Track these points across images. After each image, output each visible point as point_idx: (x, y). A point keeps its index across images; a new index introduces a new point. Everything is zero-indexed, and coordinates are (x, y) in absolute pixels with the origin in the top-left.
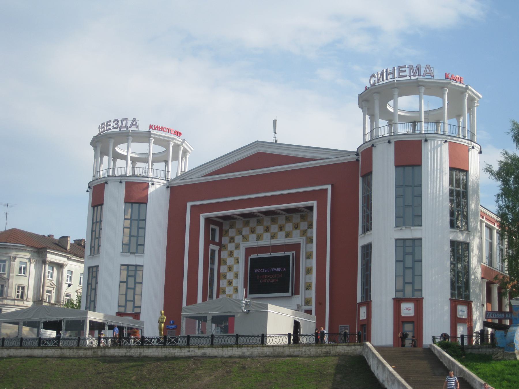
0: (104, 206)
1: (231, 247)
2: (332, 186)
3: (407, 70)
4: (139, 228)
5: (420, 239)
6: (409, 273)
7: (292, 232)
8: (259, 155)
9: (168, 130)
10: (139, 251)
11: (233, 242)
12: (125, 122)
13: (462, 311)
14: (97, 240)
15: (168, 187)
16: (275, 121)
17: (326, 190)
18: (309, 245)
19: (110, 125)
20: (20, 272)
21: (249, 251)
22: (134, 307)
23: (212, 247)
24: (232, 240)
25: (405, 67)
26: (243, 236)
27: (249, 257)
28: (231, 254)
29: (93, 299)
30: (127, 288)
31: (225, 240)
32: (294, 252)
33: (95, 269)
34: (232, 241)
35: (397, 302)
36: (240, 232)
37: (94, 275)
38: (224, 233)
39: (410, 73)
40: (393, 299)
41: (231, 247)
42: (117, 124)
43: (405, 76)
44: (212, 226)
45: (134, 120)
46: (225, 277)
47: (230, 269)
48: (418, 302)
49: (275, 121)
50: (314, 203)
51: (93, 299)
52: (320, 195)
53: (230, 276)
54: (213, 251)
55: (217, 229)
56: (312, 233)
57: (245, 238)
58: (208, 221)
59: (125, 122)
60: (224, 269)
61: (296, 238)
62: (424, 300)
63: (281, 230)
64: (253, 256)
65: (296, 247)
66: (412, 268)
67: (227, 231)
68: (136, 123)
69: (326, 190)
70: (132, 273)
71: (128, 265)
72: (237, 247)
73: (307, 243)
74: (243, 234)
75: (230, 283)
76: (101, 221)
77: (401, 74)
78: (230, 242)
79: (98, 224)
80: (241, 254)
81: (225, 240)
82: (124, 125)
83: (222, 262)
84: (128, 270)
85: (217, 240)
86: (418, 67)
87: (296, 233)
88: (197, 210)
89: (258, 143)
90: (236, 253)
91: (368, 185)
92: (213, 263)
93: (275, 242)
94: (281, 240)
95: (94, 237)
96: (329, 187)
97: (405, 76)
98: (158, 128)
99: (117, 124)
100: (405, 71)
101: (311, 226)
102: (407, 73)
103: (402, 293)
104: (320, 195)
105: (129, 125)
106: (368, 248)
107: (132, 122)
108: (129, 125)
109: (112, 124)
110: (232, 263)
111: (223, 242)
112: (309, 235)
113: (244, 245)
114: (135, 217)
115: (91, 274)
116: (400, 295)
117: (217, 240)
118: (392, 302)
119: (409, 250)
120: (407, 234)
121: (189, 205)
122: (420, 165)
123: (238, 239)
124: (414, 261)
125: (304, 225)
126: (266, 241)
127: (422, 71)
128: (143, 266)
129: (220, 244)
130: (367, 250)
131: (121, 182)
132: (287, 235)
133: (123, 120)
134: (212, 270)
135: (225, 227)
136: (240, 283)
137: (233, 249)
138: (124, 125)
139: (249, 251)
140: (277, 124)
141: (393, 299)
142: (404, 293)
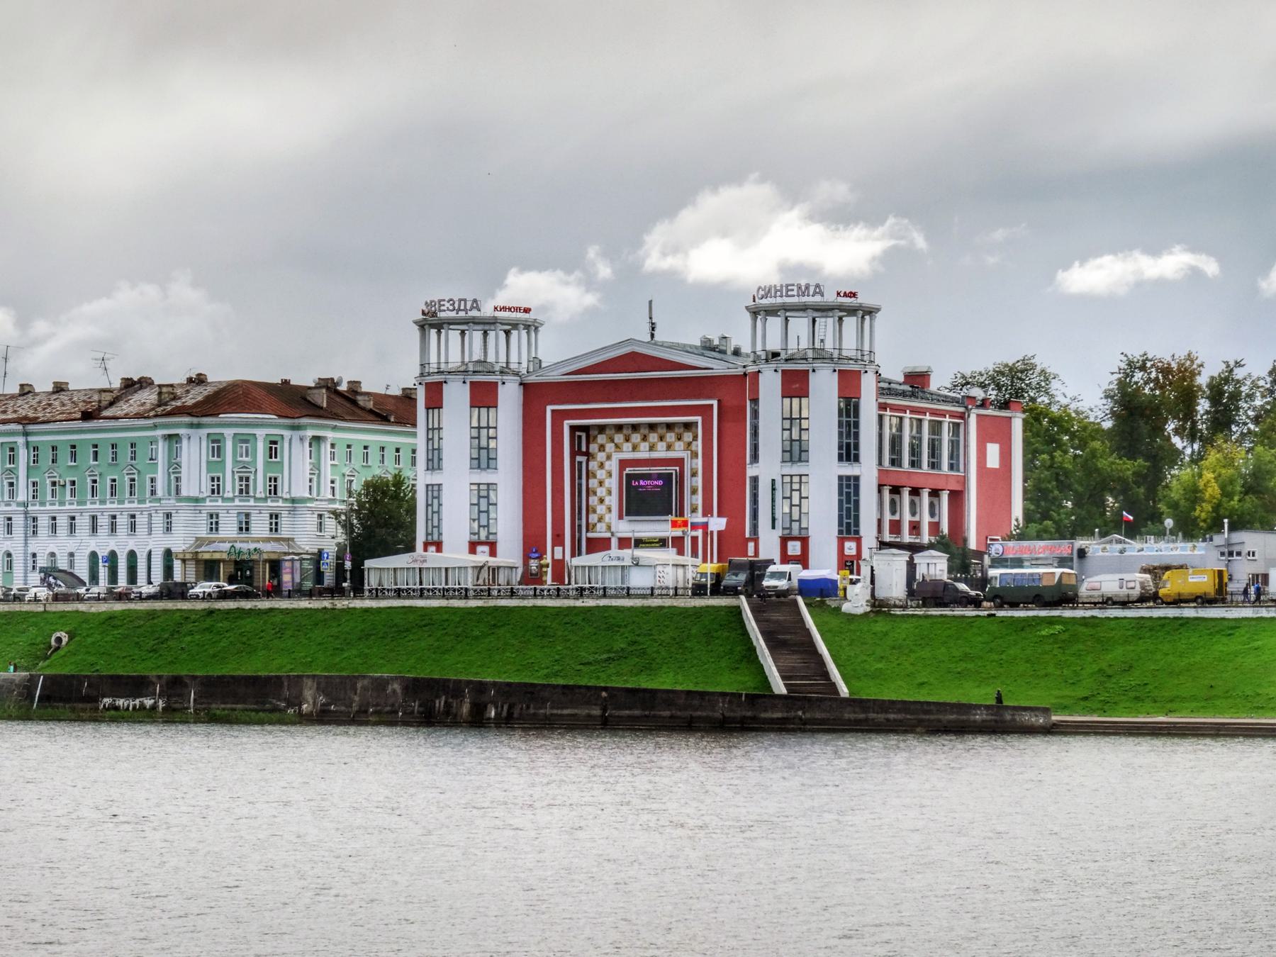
0: (444, 411)
1: (601, 456)
2: (719, 401)
3: (795, 288)
7: (674, 443)
8: (633, 355)
9: (517, 309)
11: (604, 451)
12: (463, 302)
13: (850, 548)
14: (436, 452)
15: (521, 384)
16: (650, 302)
17: (712, 405)
18: (694, 461)
19: (444, 305)
20: (271, 457)
21: (623, 464)
22: (489, 533)
23: (579, 458)
24: (602, 448)
25: (793, 285)
26: (616, 444)
27: (625, 473)
28: (602, 466)
29: (436, 524)
30: (480, 512)
31: (594, 448)
32: (677, 468)
33: (436, 488)
34: (602, 449)
35: (784, 541)
36: (612, 440)
37: (436, 494)
38: (591, 439)
39: (798, 292)
43: (794, 296)
44: (578, 433)
45: (475, 301)
46: (595, 493)
48: (804, 541)
49: (650, 302)
50: (699, 419)
51: (436, 524)
53: (601, 492)
54: (580, 463)
55: (584, 435)
56: (697, 446)
58: (573, 429)
59: (463, 302)
60: (593, 483)
61: (679, 452)
63: (661, 440)
64: (628, 470)
65: (679, 462)
67: (595, 437)
68: (477, 304)
69: (712, 405)
70: (484, 493)
71: (479, 484)
72: (609, 458)
73: (692, 458)
74: (616, 441)
75: (602, 501)
76: (439, 429)
77: (790, 293)
78: (600, 451)
79: (436, 431)
80: (613, 465)
81: (594, 448)
82: (462, 307)
83: (590, 475)
84: (479, 490)
85: (584, 449)
86: (807, 287)
87: (679, 445)
88: (559, 416)
90: (607, 464)
91: (755, 414)
92: (580, 478)
93: (655, 455)
94: (661, 453)
95: (430, 448)
96: (715, 403)
97: (794, 296)
98: (504, 309)
100: (793, 290)
101: (695, 438)
102: (795, 293)
105: (468, 308)
106: (755, 480)
107: (472, 305)
108: (468, 308)
109: (447, 305)
110: (604, 477)
111: (591, 450)
112: (694, 448)
113: (616, 457)
114: (484, 424)
115: (430, 493)
117: (584, 449)
119: (796, 486)
121: (549, 408)
123: (610, 447)
126: (643, 454)
128: (496, 484)
129: (588, 454)
130: (755, 482)
131: (464, 382)
132: (669, 447)
133: (460, 300)
134: (580, 485)
135: (593, 433)
136: (613, 501)
137: (604, 459)
138: (462, 307)
139: (623, 464)
140: (653, 303)
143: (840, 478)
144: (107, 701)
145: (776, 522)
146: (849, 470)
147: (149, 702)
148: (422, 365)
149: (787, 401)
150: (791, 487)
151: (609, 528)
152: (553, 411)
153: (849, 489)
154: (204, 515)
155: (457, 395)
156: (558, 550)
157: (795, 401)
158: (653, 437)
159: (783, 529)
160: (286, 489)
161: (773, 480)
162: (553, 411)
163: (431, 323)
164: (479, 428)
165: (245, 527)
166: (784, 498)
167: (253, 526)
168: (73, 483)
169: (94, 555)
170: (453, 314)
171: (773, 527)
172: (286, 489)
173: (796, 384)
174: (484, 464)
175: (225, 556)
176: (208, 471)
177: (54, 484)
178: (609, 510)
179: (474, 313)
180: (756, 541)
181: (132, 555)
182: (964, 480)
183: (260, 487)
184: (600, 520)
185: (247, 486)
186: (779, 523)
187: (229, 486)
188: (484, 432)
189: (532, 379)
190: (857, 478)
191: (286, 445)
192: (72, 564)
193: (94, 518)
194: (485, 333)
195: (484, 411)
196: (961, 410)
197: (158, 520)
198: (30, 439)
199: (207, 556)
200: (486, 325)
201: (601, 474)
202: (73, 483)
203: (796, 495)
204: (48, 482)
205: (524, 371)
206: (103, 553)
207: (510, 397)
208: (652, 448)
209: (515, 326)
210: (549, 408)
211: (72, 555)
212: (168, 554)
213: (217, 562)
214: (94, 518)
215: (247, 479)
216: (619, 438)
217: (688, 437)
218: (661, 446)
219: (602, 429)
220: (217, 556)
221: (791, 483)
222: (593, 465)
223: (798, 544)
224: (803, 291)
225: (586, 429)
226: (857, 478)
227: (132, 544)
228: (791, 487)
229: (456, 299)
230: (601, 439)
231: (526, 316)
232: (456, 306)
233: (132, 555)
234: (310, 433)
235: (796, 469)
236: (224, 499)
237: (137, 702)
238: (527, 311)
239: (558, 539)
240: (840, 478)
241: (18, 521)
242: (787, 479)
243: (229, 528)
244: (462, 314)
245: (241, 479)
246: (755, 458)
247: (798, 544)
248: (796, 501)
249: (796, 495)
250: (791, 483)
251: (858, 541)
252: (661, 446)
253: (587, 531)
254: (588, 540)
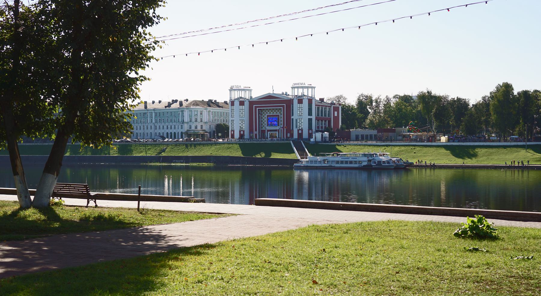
1: (264, 114)
16: (273, 86)
21: (268, 116)
23: (260, 115)
24: (264, 113)
28: (264, 116)
31: (262, 113)
35: (298, 130)
41: (264, 114)
45: (240, 86)
47: (264, 120)
48: (302, 130)
49: (273, 86)
50: (282, 108)
52: (283, 106)
54: (260, 116)
57: (267, 113)
65: (278, 116)
67: (262, 111)
70: (242, 122)
72: (265, 115)
80: (266, 116)
81: (262, 113)
87: (278, 112)
89: (269, 93)
90: (265, 116)
91: (293, 107)
93: (274, 114)
96: (285, 105)
98: (245, 87)
101: (281, 111)
104: (283, 106)
106: (293, 119)
113: (267, 115)
114: (242, 109)
119: (300, 120)
121: (254, 106)
123: (265, 113)
125: (280, 111)
127: (303, 84)
132: (276, 113)
139: (268, 116)
143: (309, 119)
144: (174, 161)
146: (310, 117)
147: (182, 161)
148: (230, 98)
149: (299, 104)
151: (265, 128)
152: (255, 106)
153: (310, 120)
154: (189, 126)
155: (237, 103)
156: (256, 132)
157: (300, 104)
158: (273, 111)
160: (204, 120)
161: (296, 119)
162: (255, 106)
163: (231, 90)
165: (196, 127)
167: (198, 128)
168: (163, 119)
169: (167, 133)
170: (236, 88)
172: (204, 120)
173: (300, 101)
175: (193, 133)
176: (189, 117)
177: (160, 120)
178: (265, 124)
179: (240, 88)
180: (293, 130)
181: (175, 133)
182: (331, 119)
183: (199, 120)
184: (264, 126)
185: (196, 120)
187: (193, 120)
189: (251, 100)
190: (312, 119)
191: (204, 112)
192: (163, 134)
193: (167, 126)
194: (242, 92)
196: (330, 105)
197: (180, 127)
198: (155, 111)
199: (189, 133)
200: (242, 90)
201: (264, 118)
202: (163, 119)
203: (300, 122)
204: (159, 119)
205: (249, 99)
206: (169, 133)
207: (247, 104)
208: (273, 113)
209: (248, 90)
210: (254, 106)
211: (163, 133)
212: (182, 133)
213: (191, 134)
214: (167, 126)
215: (197, 119)
216: (267, 111)
217: (280, 111)
218: (275, 113)
219: (264, 109)
220: (191, 133)
222: (262, 116)
223: (301, 131)
224: (302, 84)
225: (261, 109)
226: (312, 119)
227: (175, 131)
230: (264, 111)
231: (249, 88)
233: (175, 133)
234: (208, 110)
236: (192, 123)
237: (180, 161)
238: (249, 87)
239: (256, 130)
240: (309, 119)
241: (153, 127)
242: (299, 119)
243: (193, 128)
244: (238, 88)
245: (195, 119)
246: (293, 115)
247: (301, 131)
249: (300, 122)
251: (312, 130)
252: (275, 113)
253: (261, 128)
254: (262, 130)
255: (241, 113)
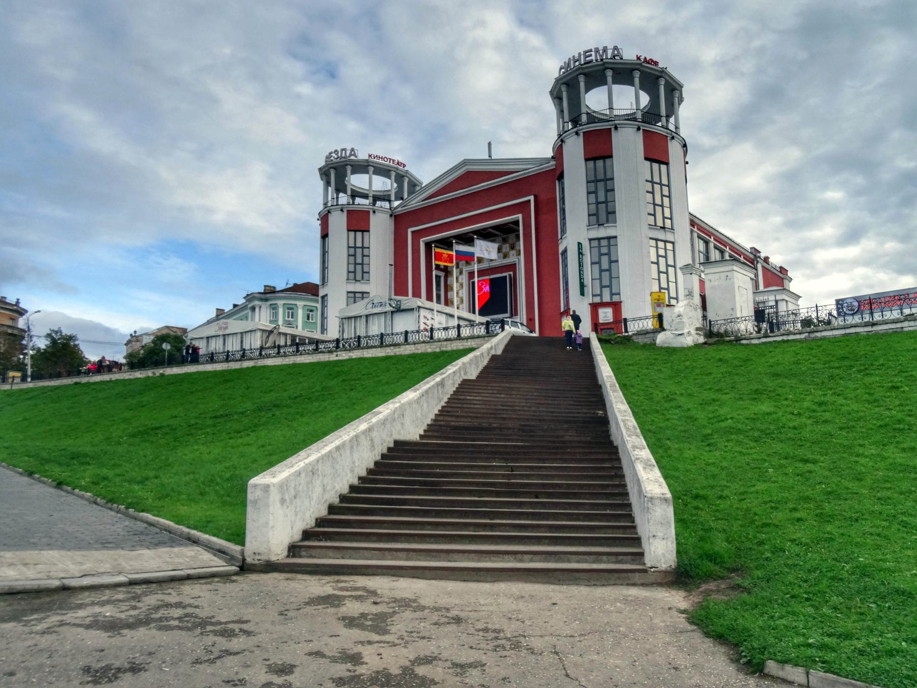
3: (593, 53)
4: (363, 256)
5: (615, 237)
6: (606, 275)
10: (365, 278)
35: (595, 307)
40: (590, 304)
42: (337, 154)
45: (352, 150)
48: (616, 306)
62: (622, 304)
66: (609, 270)
71: (355, 293)
77: (588, 59)
82: (343, 155)
99: (337, 154)
100: (591, 55)
103: (599, 298)
105: (348, 155)
107: (351, 153)
109: (334, 155)
114: (359, 244)
116: (597, 300)
118: (589, 306)
119: (604, 250)
120: (602, 232)
122: (611, 157)
124: (611, 262)
133: (342, 150)
141: (590, 304)
142: (601, 298)
145: (585, 288)
150: (600, 251)
159: (594, 296)
161: (579, 244)
164: (355, 247)
166: (592, 263)
171: (582, 294)
174: (359, 276)
186: (588, 290)
188: (359, 251)
195: (359, 234)
203: (605, 260)
221: (599, 247)
228: (600, 251)
229: (339, 150)
232: (339, 154)
235: (602, 232)
246: (564, 231)
248: (605, 265)
249: (605, 260)
250: (599, 247)
255: (356, 264)
